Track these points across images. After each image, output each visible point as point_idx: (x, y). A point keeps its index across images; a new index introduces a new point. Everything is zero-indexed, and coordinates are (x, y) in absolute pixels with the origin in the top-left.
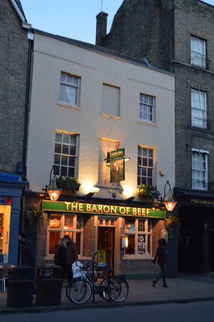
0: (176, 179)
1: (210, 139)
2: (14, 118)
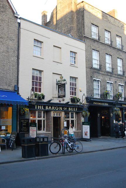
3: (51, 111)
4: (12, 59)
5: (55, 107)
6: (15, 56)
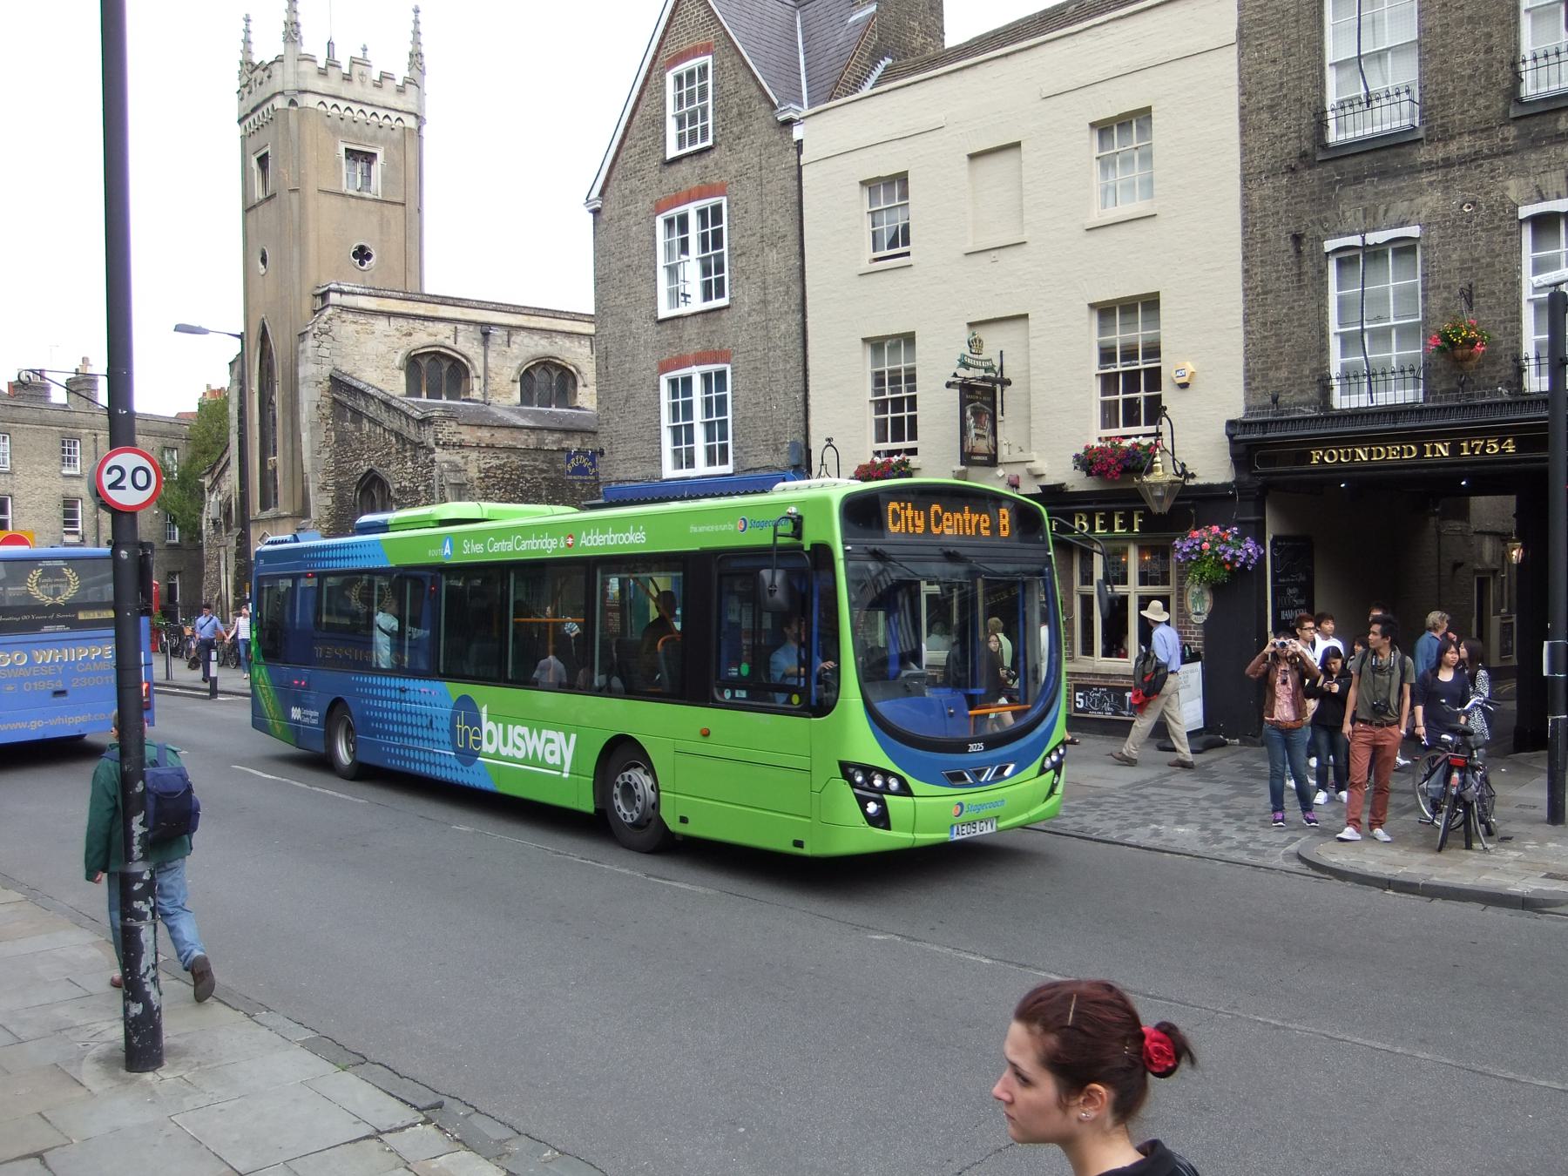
0: (1247, 384)
1: (1430, 166)
4: (783, 327)
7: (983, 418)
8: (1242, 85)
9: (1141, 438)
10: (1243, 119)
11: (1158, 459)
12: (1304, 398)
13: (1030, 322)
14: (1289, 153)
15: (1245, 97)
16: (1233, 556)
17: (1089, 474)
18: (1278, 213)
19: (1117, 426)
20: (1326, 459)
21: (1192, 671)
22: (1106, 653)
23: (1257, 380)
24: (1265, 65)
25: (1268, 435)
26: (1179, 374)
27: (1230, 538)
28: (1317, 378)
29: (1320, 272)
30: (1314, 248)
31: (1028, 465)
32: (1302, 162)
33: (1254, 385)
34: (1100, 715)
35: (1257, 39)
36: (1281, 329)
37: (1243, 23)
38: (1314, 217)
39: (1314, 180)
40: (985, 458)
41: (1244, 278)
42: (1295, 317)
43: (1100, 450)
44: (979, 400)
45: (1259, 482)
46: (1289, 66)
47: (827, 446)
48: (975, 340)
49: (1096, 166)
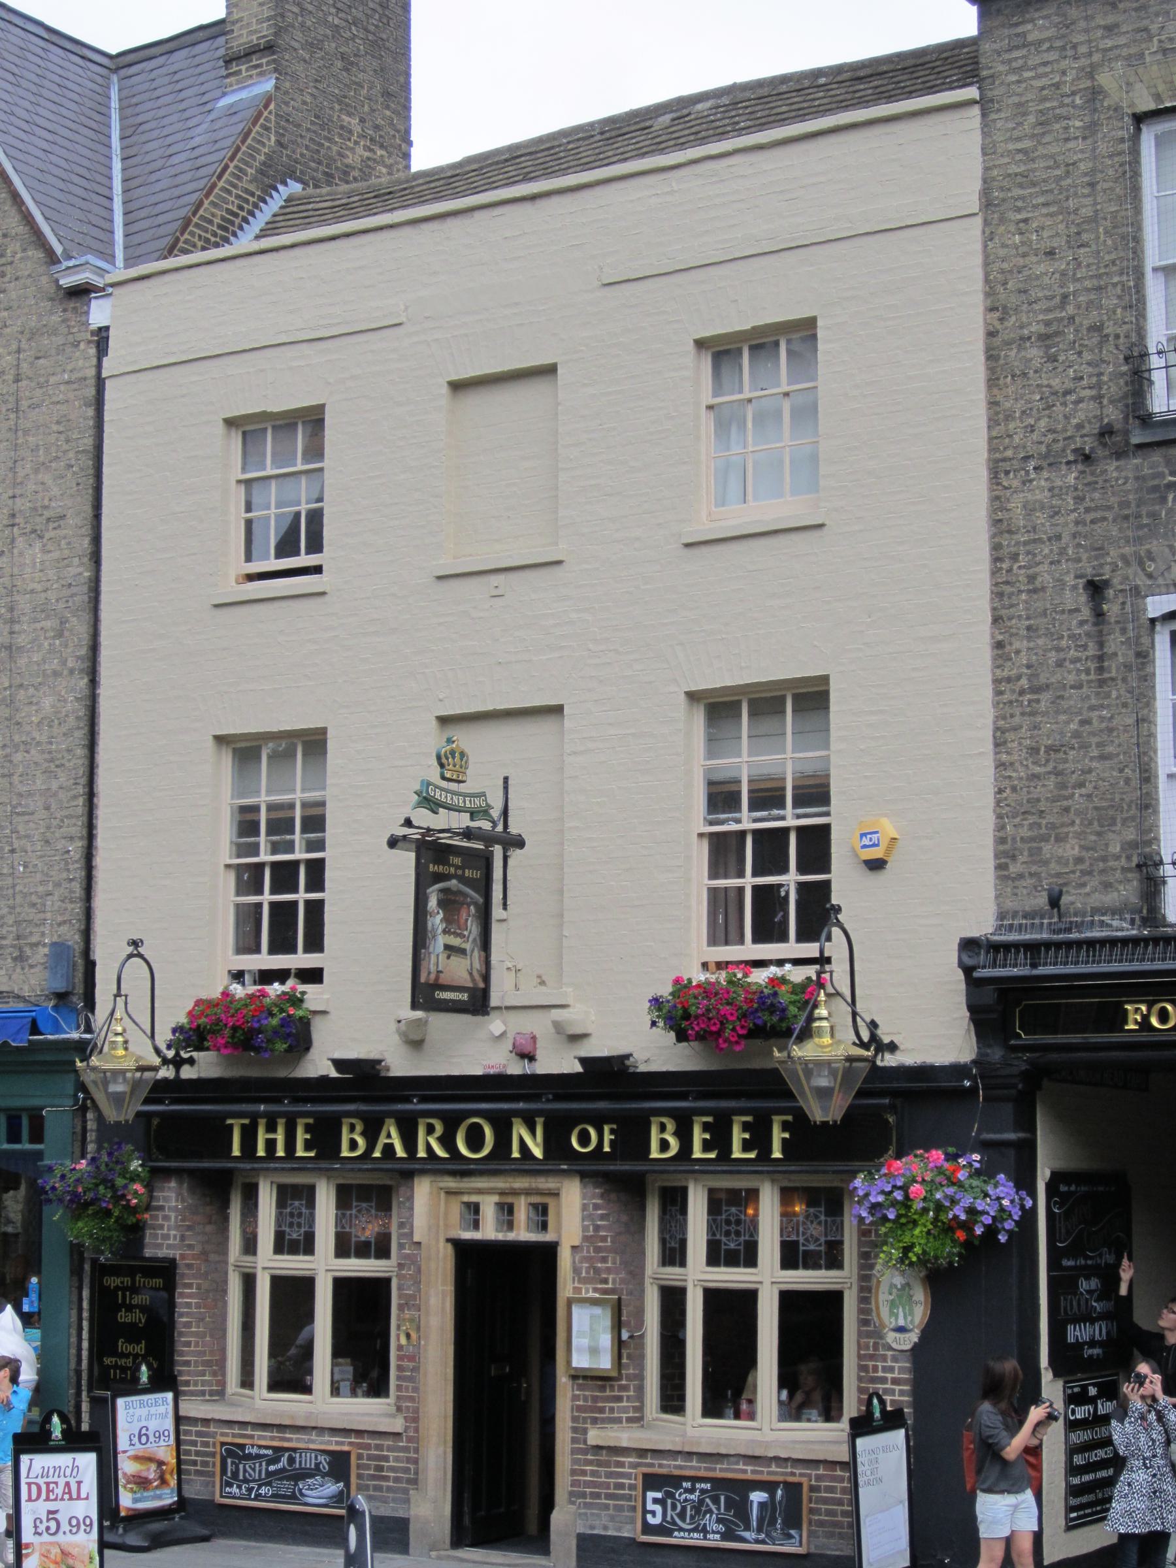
2: (44, 739)
3: (408, 1176)
4: (47, 703)
5: (451, 1123)
6: (70, 664)
7: (464, 915)
8: (990, 293)
9: (788, 966)
10: (991, 356)
11: (822, 1012)
12: (1110, 899)
13: (568, 723)
14: (1079, 426)
15: (997, 314)
16: (972, 1211)
17: (682, 1036)
18: (1058, 537)
19: (741, 941)
20: (1154, 1022)
21: (886, 1449)
22: (712, 1408)
23: (1021, 859)
24: (1034, 259)
25: (1042, 970)
26: (866, 841)
27: (962, 1175)
28: (1135, 860)
29: (1139, 655)
30: (1128, 608)
31: (556, 1014)
32: (1105, 445)
33: (1014, 869)
34: (696, 1540)
35: (1019, 210)
36: (1066, 761)
37: (993, 179)
38: (1127, 550)
39: (1127, 479)
40: (465, 997)
41: (995, 658)
42: (1094, 740)
43: (707, 990)
44: (455, 876)
45: (1021, 1063)
46: (1079, 265)
47: (130, 956)
48: (453, 753)
49: (707, 423)
